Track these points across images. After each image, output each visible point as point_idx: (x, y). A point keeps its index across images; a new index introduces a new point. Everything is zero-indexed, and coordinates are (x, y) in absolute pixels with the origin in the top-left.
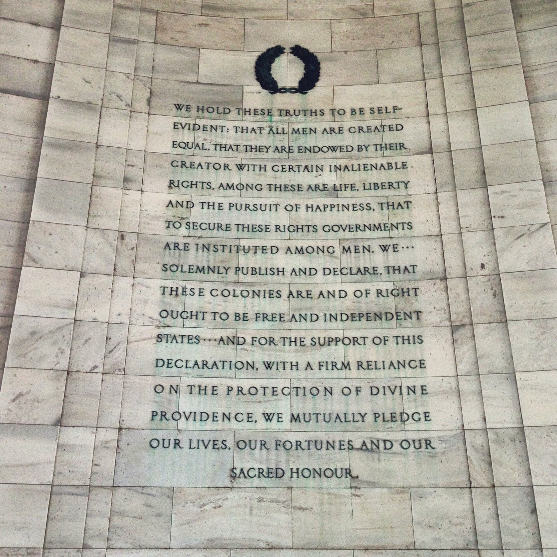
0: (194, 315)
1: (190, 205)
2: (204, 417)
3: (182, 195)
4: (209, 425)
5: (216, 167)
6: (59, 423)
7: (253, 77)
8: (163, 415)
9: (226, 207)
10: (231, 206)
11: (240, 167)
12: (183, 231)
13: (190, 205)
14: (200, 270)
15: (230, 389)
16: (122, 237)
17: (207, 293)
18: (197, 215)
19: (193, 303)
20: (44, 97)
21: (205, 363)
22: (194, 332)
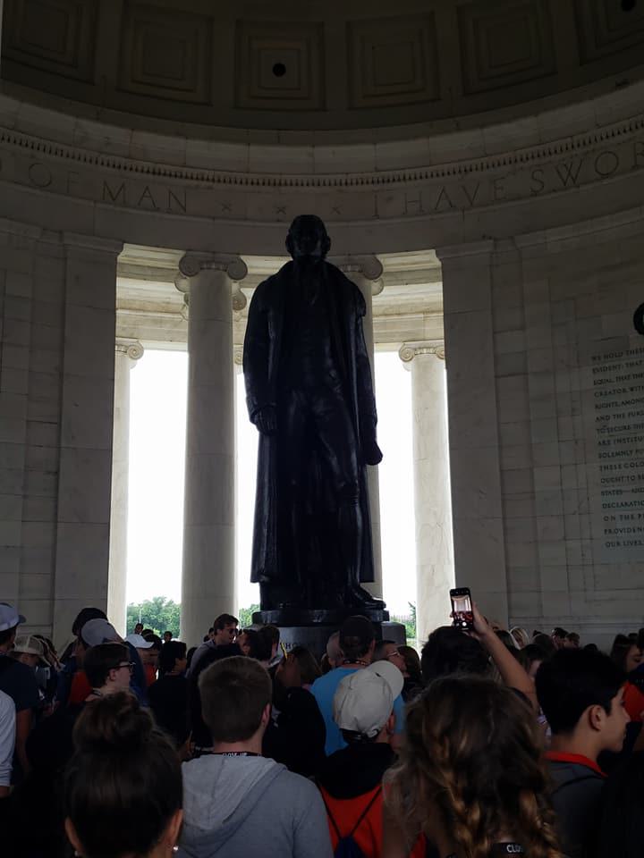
0: (618, 479)
1: (608, 418)
2: (629, 530)
3: (604, 412)
4: (632, 534)
5: (619, 391)
6: (565, 539)
7: (633, 328)
8: (610, 531)
9: (626, 415)
10: (629, 414)
11: (632, 390)
12: (607, 434)
13: (608, 418)
14: (618, 454)
15: (640, 515)
16: (576, 443)
17: (622, 466)
18: (612, 423)
19: (616, 473)
20: (526, 374)
21: (626, 504)
22: (619, 488)
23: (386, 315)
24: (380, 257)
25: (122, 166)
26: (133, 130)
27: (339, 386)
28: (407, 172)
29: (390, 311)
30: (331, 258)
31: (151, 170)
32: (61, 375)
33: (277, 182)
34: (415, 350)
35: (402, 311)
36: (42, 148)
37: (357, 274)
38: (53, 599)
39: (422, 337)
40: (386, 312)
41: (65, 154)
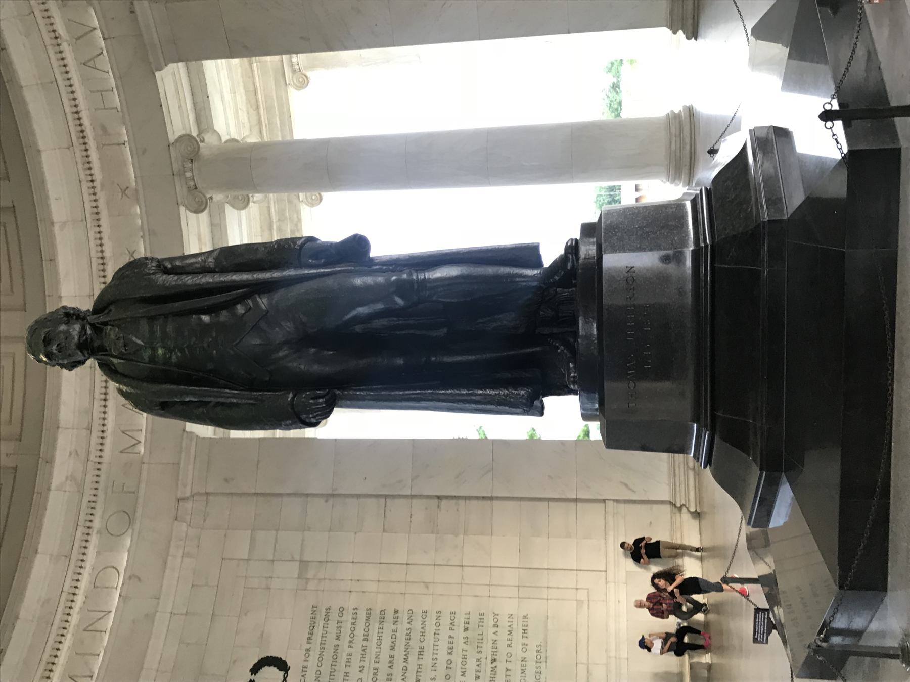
23: (258, 107)
24: (172, 138)
25: (101, 434)
26: (58, 428)
27: (259, 299)
28: (68, 109)
29: (253, 101)
30: (86, 305)
31: (103, 403)
32: (333, 495)
33: (101, 261)
34: (294, 71)
35: (252, 89)
36: (89, 524)
37: (195, 165)
38: (576, 500)
39: (279, 63)
40: (254, 107)
41: (94, 498)
